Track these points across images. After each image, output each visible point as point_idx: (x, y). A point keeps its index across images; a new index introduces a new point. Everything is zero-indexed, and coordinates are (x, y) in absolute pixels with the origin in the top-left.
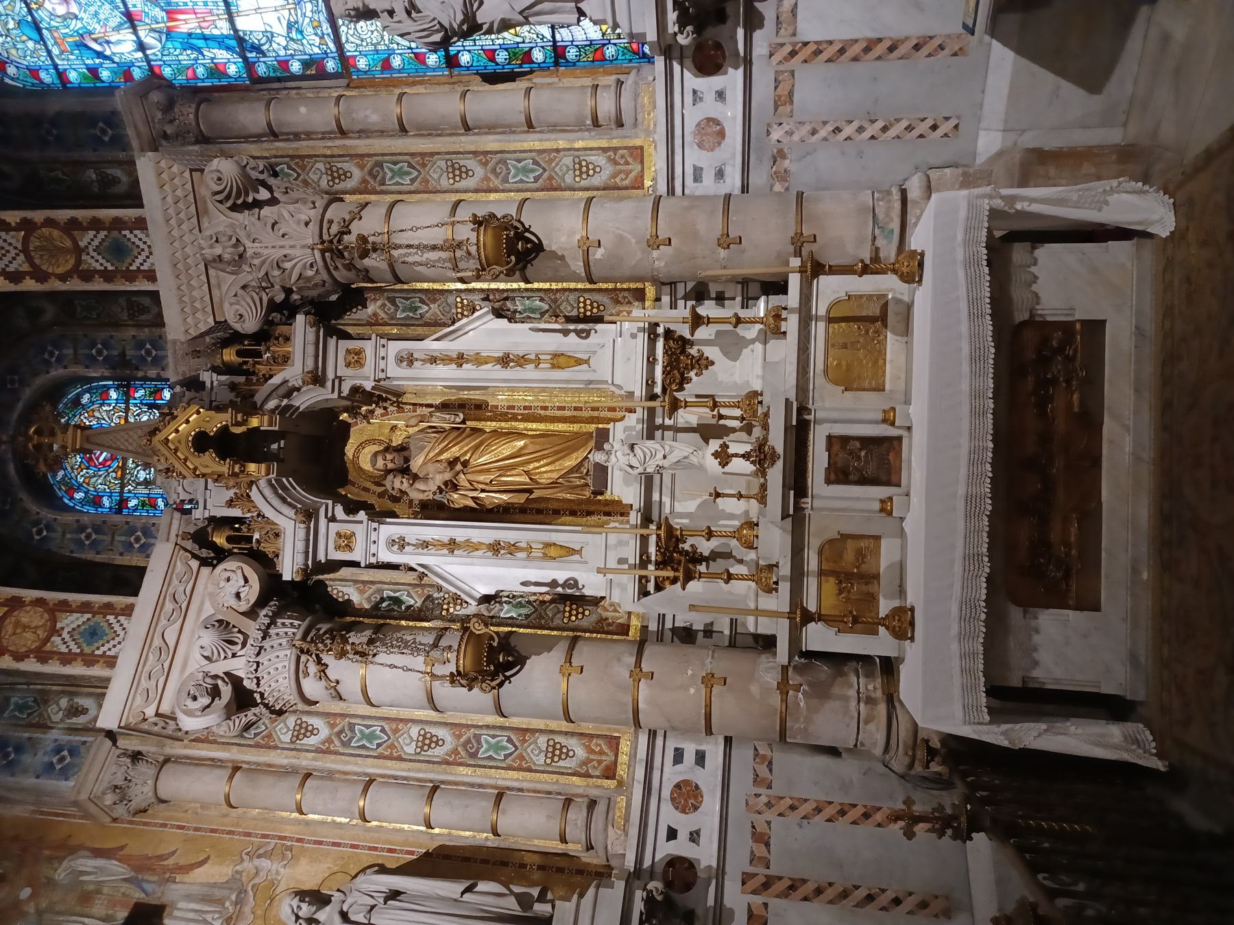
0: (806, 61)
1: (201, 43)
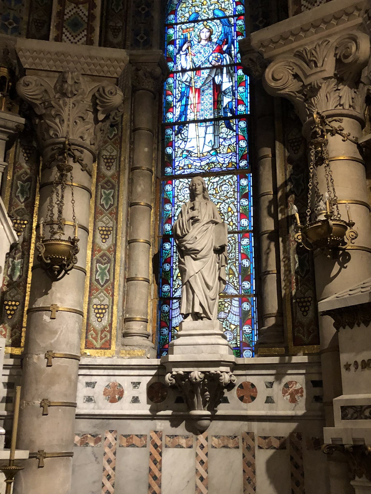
0: (151, 454)
1: (184, 102)
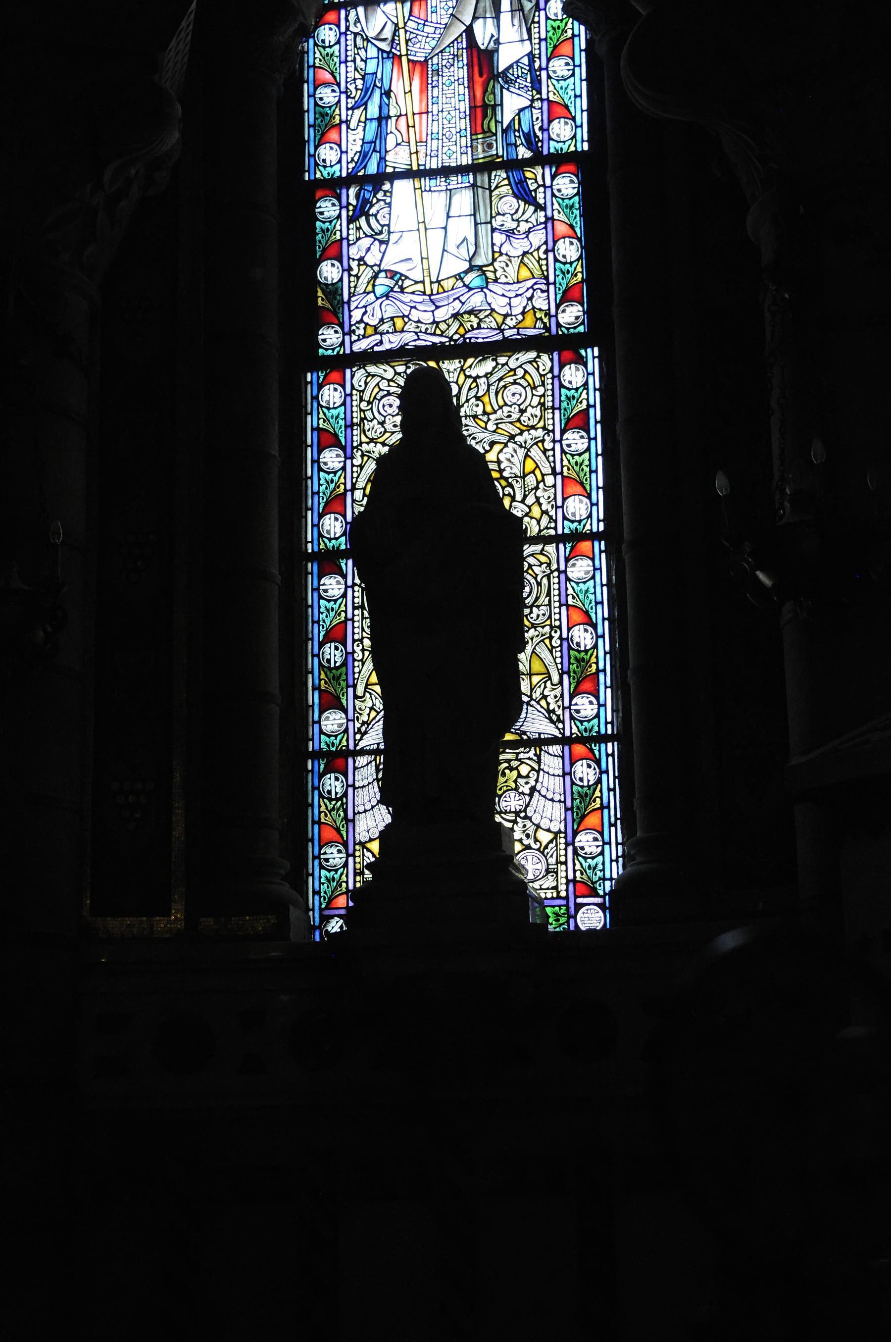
1: (373, 110)
